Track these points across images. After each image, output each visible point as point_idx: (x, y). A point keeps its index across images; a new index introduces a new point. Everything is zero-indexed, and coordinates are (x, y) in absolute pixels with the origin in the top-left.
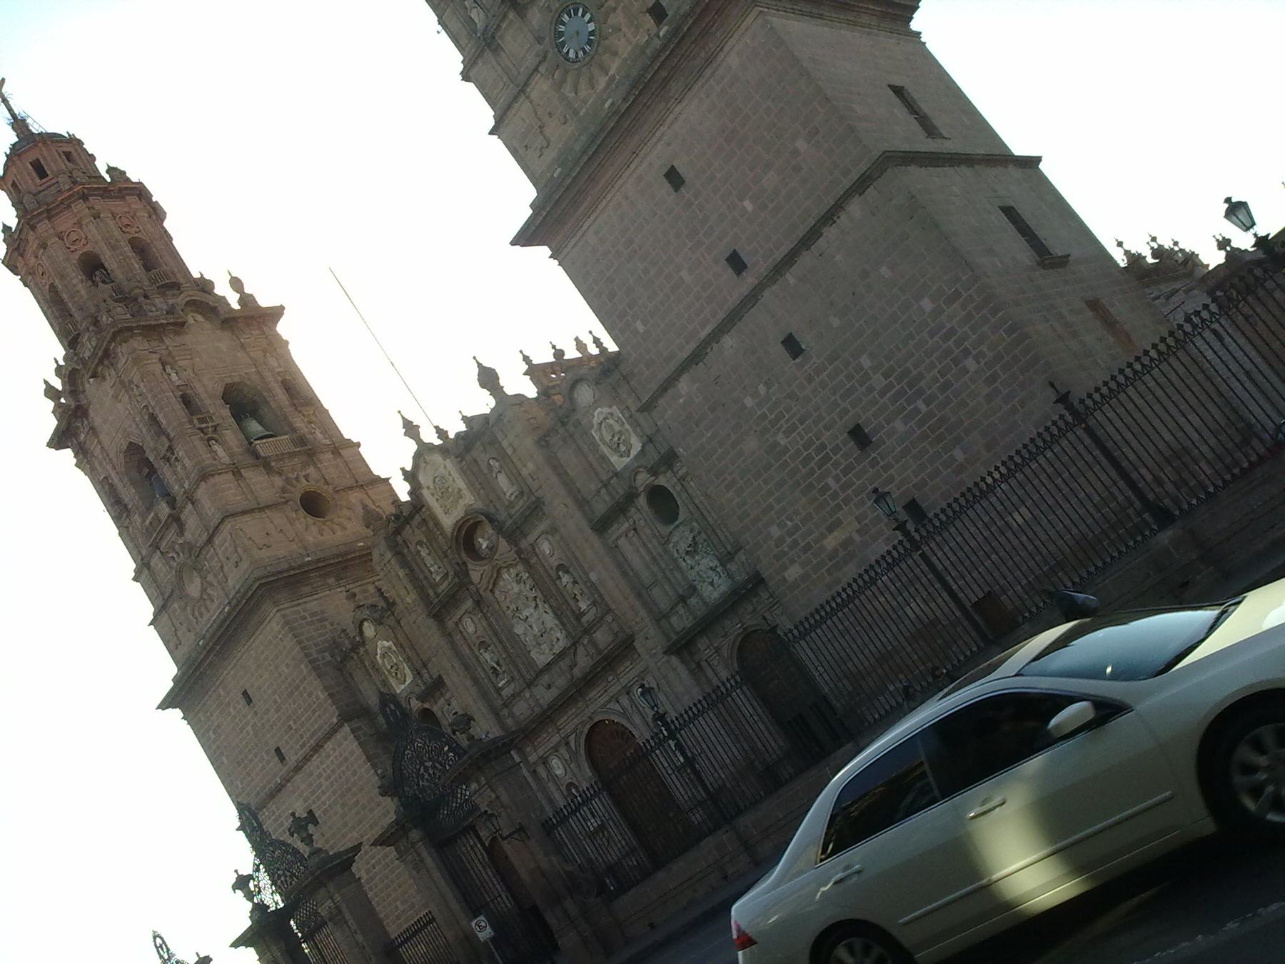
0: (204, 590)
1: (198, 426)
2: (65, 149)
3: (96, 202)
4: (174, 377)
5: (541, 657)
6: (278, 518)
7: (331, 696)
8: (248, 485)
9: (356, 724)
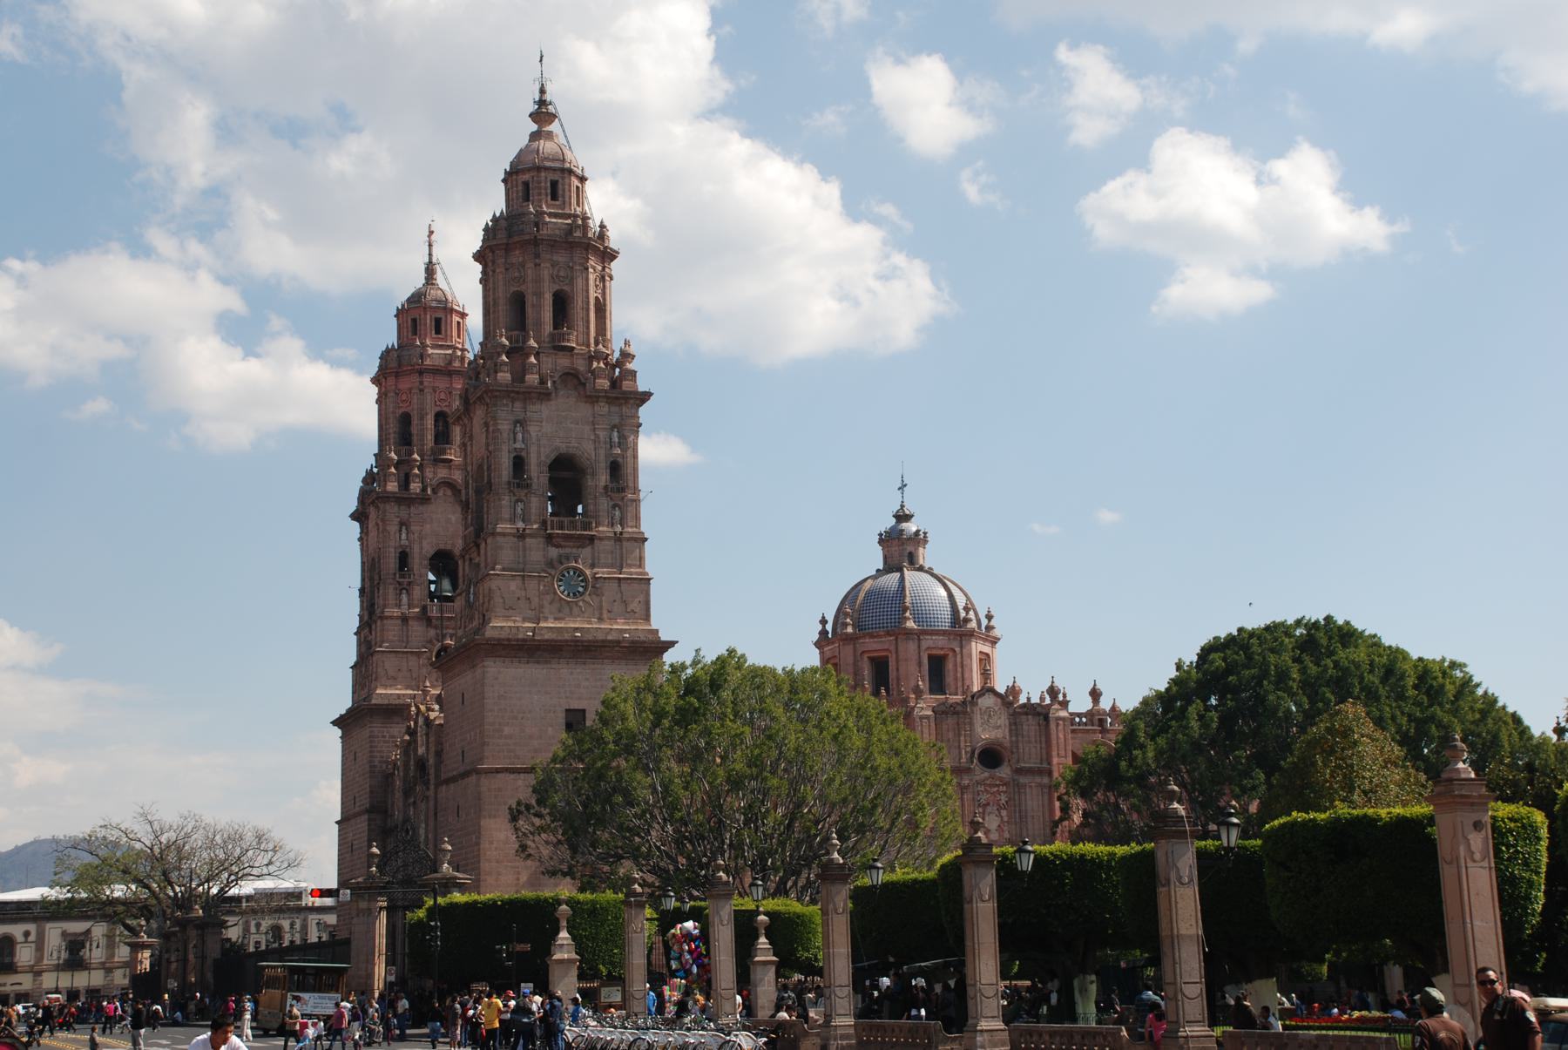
1: (398, 579)
2: (440, 314)
3: (427, 380)
4: (404, 536)
6: (413, 661)
7: (371, 792)
8: (408, 631)
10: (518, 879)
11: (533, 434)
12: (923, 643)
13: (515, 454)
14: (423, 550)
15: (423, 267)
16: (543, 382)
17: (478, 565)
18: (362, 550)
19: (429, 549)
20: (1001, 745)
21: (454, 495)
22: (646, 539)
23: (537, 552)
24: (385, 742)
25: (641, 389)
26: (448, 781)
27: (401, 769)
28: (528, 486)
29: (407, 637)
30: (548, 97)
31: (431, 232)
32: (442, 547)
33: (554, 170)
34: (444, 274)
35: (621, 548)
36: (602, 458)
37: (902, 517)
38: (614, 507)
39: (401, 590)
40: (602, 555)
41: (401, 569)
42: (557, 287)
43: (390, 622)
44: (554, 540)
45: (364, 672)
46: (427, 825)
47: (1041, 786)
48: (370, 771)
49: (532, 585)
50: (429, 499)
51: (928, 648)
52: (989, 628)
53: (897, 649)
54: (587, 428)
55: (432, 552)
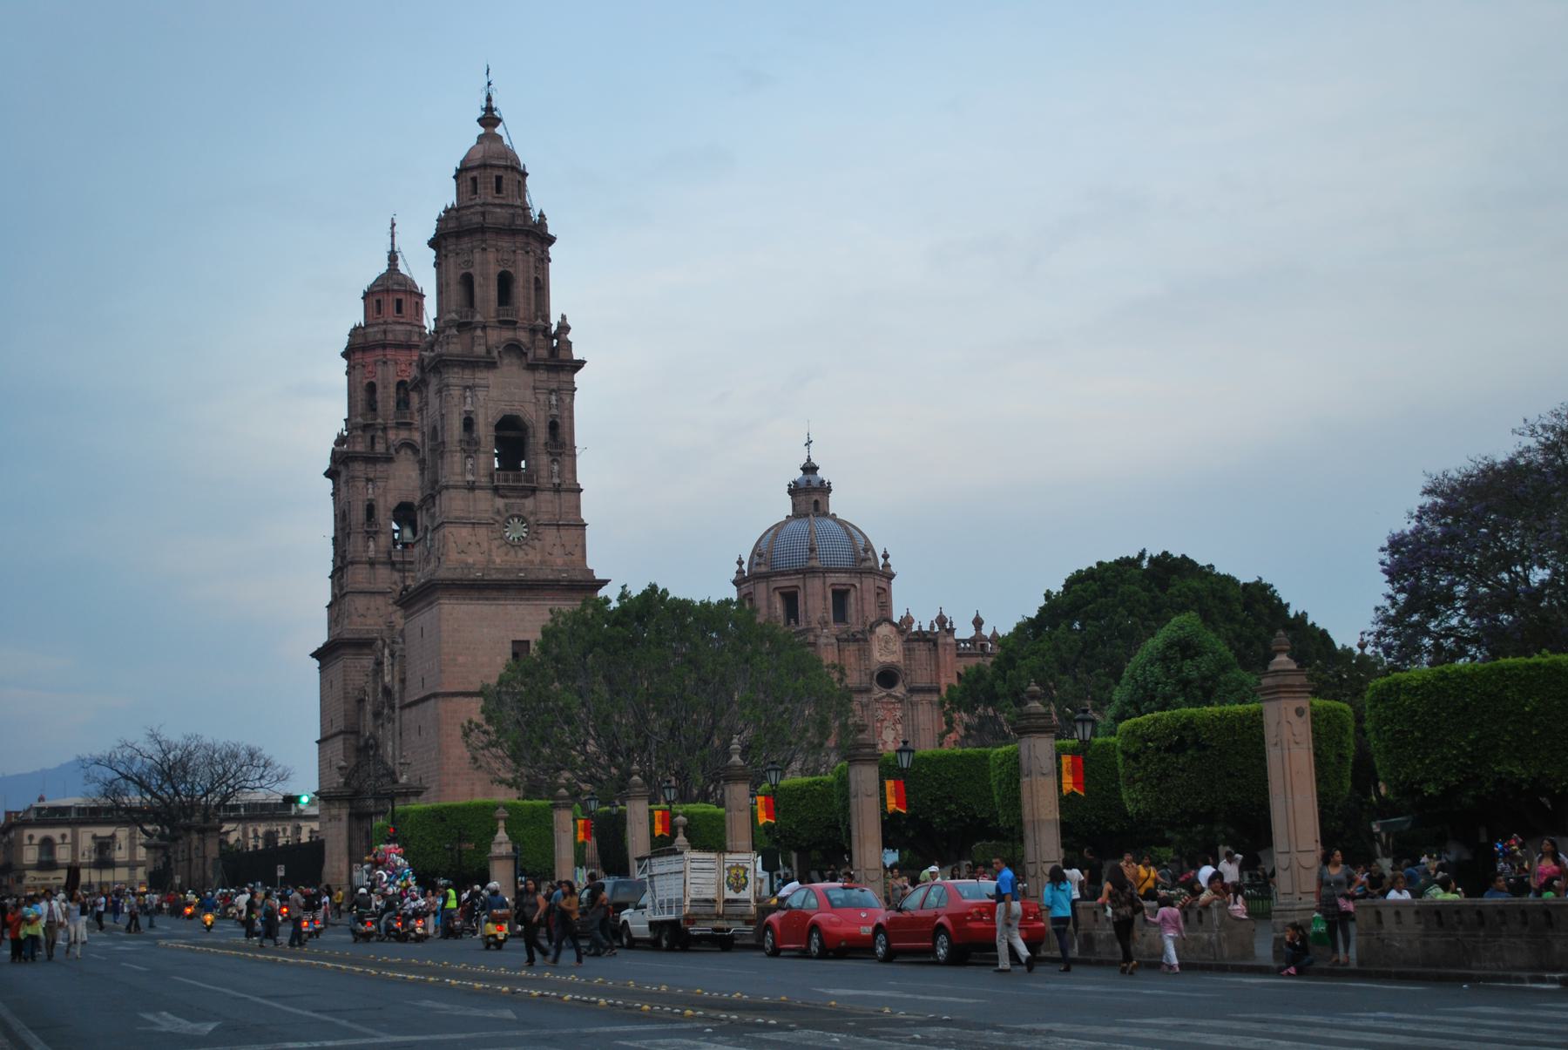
0: (338, 616)
2: (400, 296)
3: (390, 353)
4: (370, 491)
6: (380, 600)
7: (345, 715)
9: (348, 736)
10: (472, 790)
11: (481, 398)
12: (828, 579)
13: (465, 416)
14: (387, 502)
15: (387, 255)
16: (489, 352)
17: (434, 513)
18: (335, 503)
19: (393, 501)
20: (896, 668)
21: (414, 453)
23: (485, 504)
25: (576, 356)
26: (410, 705)
27: (371, 694)
28: (477, 443)
30: (494, 105)
31: (393, 225)
32: (404, 500)
33: (498, 167)
34: (404, 260)
35: (560, 499)
36: (542, 418)
37: (810, 469)
42: (501, 269)
44: (501, 492)
46: (394, 743)
47: (931, 703)
48: (345, 698)
49: (482, 532)
51: (832, 584)
52: (886, 565)
53: (805, 585)
54: (529, 394)
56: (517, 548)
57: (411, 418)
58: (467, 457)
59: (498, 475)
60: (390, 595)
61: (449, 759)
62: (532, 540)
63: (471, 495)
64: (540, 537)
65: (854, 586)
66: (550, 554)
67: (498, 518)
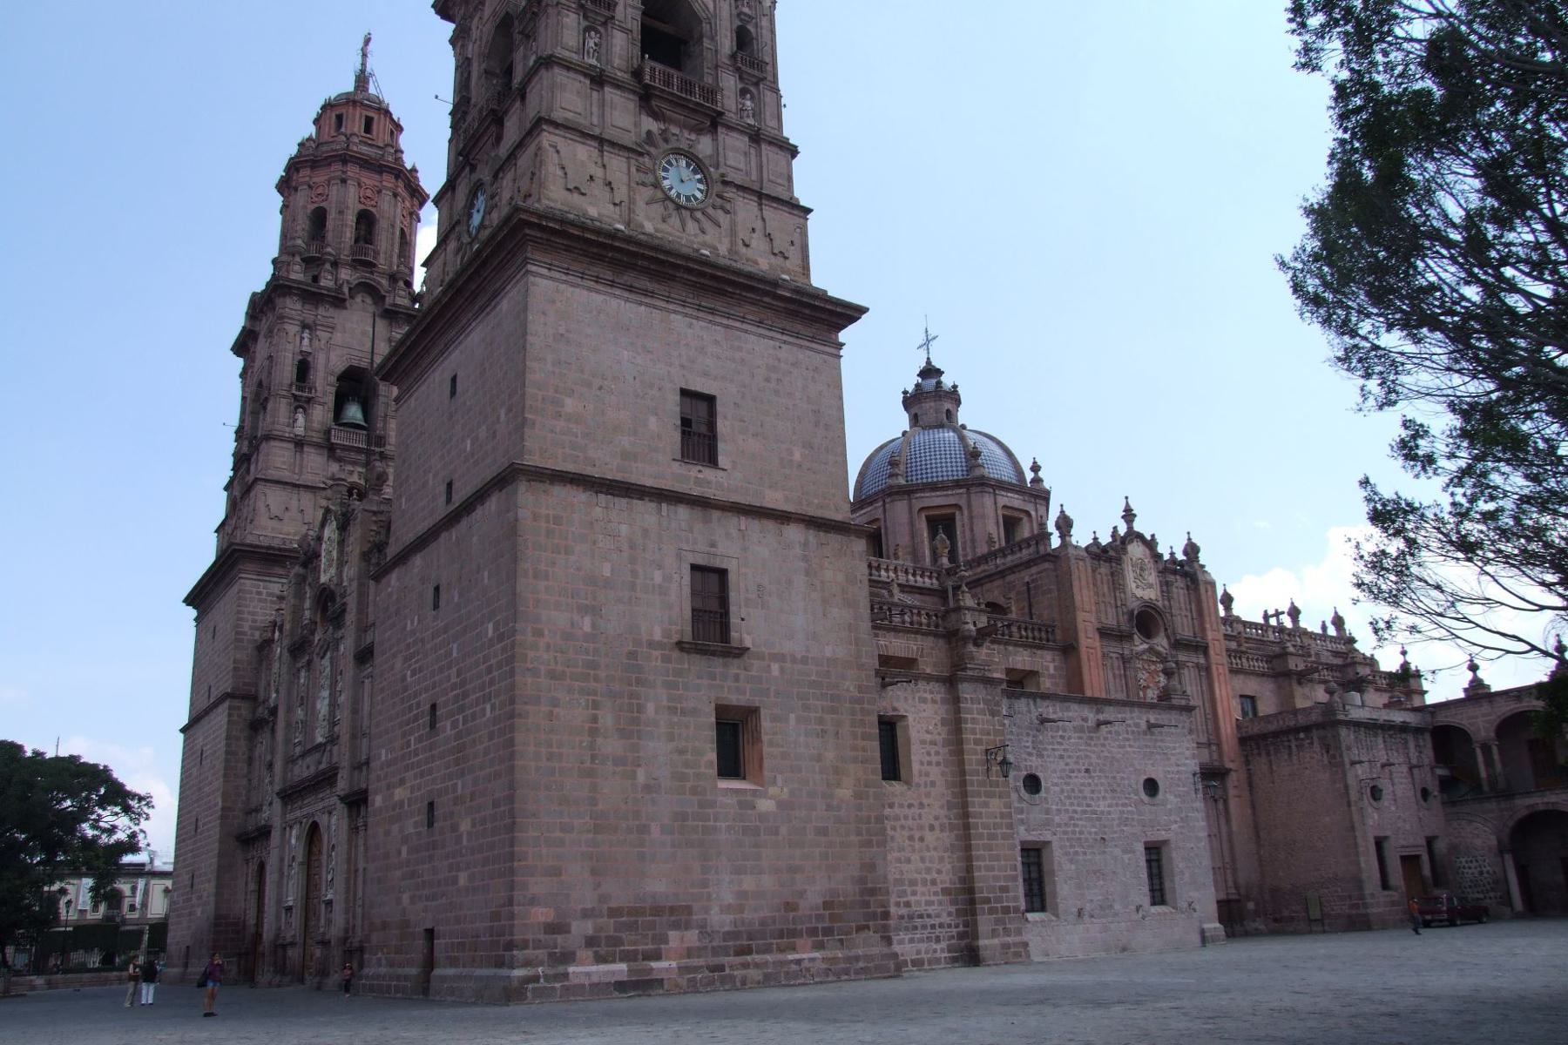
2: (370, 114)
3: (352, 170)
4: (306, 342)
5: (320, 740)
6: (307, 499)
7: (235, 669)
8: (302, 459)
9: (236, 703)
10: (595, 719)
12: (999, 498)
20: (1155, 608)
21: (375, 303)
22: (793, 152)
24: (260, 600)
29: (301, 467)
31: (367, 41)
32: (355, 363)
37: (930, 372)
38: (743, 92)
39: (296, 408)
40: (730, 154)
41: (299, 379)
43: (277, 444)
45: (242, 487)
47: (1197, 666)
49: (618, 165)
50: (345, 300)
51: (1004, 507)
53: (969, 506)
55: (340, 366)
56: (686, 214)
57: (375, 258)
58: (587, 30)
59: (653, 69)
60: (324, 493)
61: (539, 633)
62: (714, 207)
63: (595, 94)
64: (728, 206)
65: (1028, 513)
66: (746, 245)
67: (647, 147)
